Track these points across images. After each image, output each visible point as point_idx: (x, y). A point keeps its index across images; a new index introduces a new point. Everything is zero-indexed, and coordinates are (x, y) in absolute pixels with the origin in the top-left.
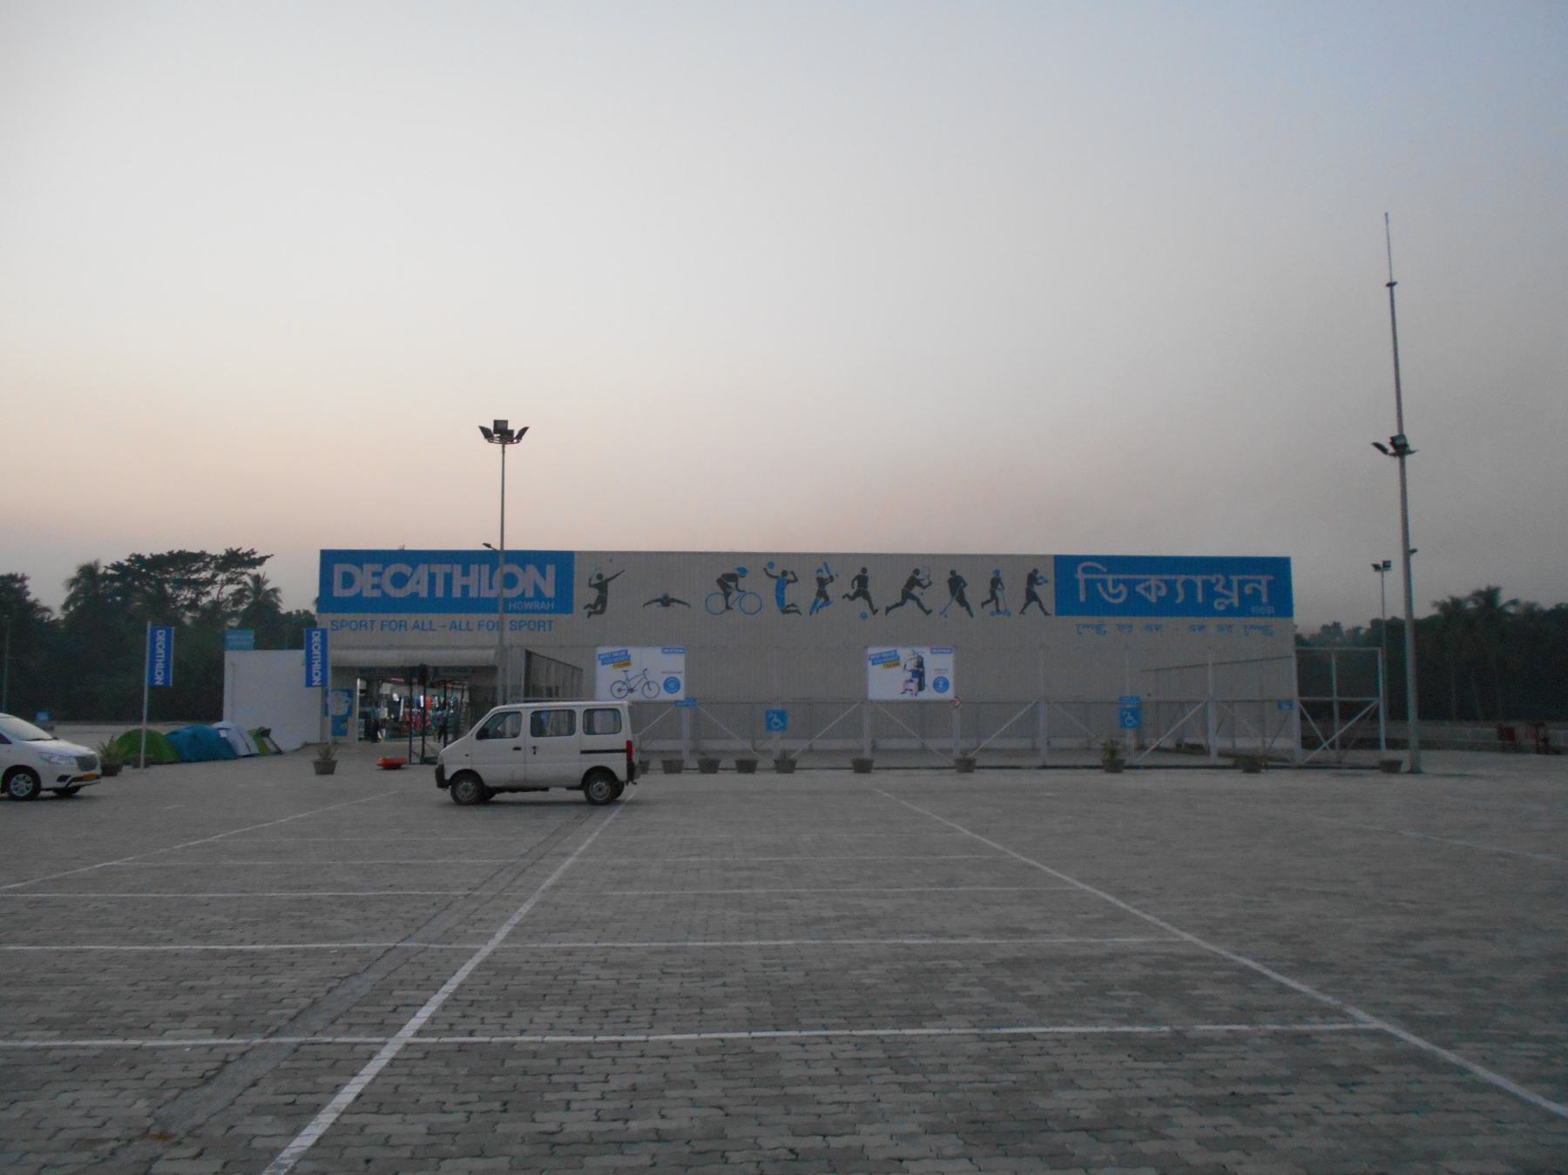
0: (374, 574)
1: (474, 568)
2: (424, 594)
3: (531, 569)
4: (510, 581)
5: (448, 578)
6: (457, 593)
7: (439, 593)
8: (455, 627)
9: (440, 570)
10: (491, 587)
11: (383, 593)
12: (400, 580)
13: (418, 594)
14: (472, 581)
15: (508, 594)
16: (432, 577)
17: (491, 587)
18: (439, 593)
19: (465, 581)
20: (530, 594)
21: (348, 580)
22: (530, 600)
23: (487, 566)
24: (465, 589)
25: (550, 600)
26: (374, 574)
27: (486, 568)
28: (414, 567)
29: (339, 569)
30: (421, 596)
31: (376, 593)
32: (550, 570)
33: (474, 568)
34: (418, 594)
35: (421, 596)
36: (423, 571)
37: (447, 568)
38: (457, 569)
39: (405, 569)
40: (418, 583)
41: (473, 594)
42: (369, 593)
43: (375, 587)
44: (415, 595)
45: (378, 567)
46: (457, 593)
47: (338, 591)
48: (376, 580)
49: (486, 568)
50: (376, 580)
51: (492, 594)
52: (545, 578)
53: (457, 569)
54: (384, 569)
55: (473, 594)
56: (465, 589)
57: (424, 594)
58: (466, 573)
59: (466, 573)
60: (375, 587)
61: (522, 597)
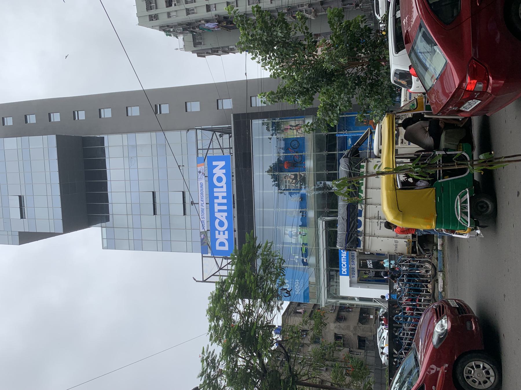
0: (219, 234)
2: (225, 214)
3: (214, 171)
4: (220, 179)
5: (219, 204)
6: (225, 201)
7: (225, 208)
9: (217, 208)
10: (222, 187)
11: (226, 230)
12: (221, 224)
14: (220, 195)
16: (220, 211)
17: (222, 187)
18: (225, 208)
19: (220, 197)
21: (222, 244)
24: (223, 198)
26: (219, 234)
27: (215, 190)
29: (218, 248)
30: (227, 215)
31: (226, 232)
32: (215, 163)
33: (216, 194)
35: (227, 215)
36: (217, 215)
37: (216, 205)
39: (217, 221)
40: (222, 216)
41: (225, 194)
42: (226, 236)
43: (224, 234)
45: (217, 232)
46: (225, 201)
47: (226, 248)
48: (222, 233)
49: (215, 190)
50: (222, 233)
54: (217, 230)
55: (225, 194)
56: (223, 198)
57: (225, 214)
58: (217, 198)
59: (217, 198)
60: (224, 234)
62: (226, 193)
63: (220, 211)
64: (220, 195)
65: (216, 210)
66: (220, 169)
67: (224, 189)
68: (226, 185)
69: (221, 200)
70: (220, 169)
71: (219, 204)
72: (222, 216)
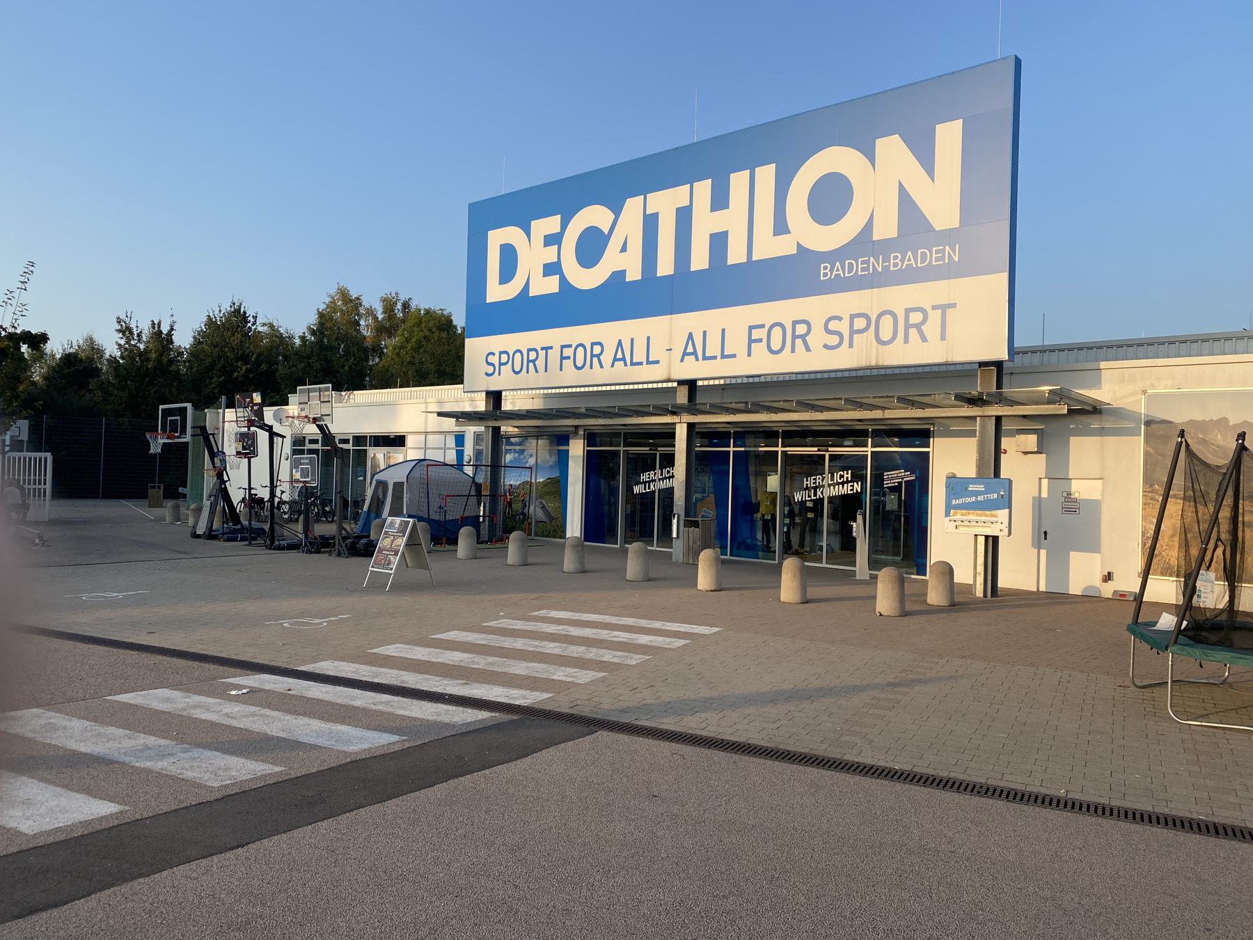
5: (684, 216)
6: (700, 259)
8: (695, 353)
9: (665, 202)
10: (781, 227)
11: (563, 281)
14: (732, 220)
15: (826, 238)
16: (651, 223)
17: (781, 227)
20: (886, 228)
22: (886, 247)
24: (719, 242)
25: (947, 237)
28: (617, 211)
40: (624, 249)
41: (736, 255)
44: (619, 275)
45: (551, 224)
46: (700, 259)
48: (550, 255)
50: (550, 255)
51: (783, 247)
52: (930, 170)
54: (564, 225)
56: (719, 242)
58: (720, 201)
59: (720, 201)
61: (863, 242)
63: (651, 223)
66: (901, 186)
67: (769, 247)
69: (705, 224)
70: (901, 186)
71: (684, 216)
72: (624, 249)
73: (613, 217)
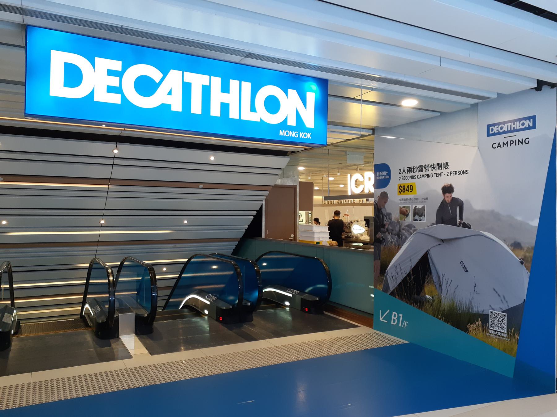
1: (234, 84)
2: (177, 106)
5: (206, 91)
6: (215, 111)
7: (196, 108)
10: (253, 109)
13: (170, 105)
14: (231, 98)
16: (187, 88)
17: (253, 109)
18: (196, 108)
19: (225, 98)
23: (249, 84)
24: (225, 107)
33: (234, 84)
34: (170, 105)
37: (204, 79)
38: (216, 82)
40: (170, 93)
41: (233, 114)
44: (166, 107)
46: (215, 111)
53: (216, 82)
55: (233, 114)
56: (225, 107)
57: (177, 106)
58: (225, 89)
59: (225, 89)
62: (238, 118)
63: (187, 88)
64: (231, 98)
65: (190, 77)
67: (247, 116)
68: (260, 121)
71: (206, 91)
72: (170, 93)
73: (162, 75)
